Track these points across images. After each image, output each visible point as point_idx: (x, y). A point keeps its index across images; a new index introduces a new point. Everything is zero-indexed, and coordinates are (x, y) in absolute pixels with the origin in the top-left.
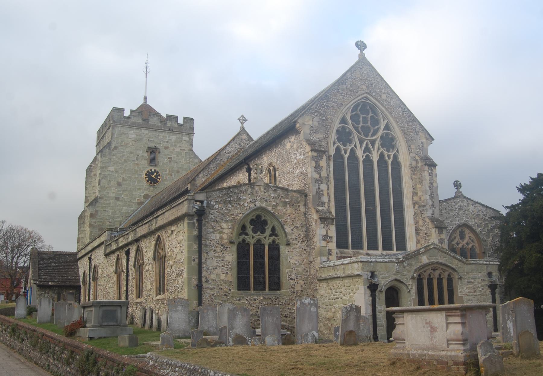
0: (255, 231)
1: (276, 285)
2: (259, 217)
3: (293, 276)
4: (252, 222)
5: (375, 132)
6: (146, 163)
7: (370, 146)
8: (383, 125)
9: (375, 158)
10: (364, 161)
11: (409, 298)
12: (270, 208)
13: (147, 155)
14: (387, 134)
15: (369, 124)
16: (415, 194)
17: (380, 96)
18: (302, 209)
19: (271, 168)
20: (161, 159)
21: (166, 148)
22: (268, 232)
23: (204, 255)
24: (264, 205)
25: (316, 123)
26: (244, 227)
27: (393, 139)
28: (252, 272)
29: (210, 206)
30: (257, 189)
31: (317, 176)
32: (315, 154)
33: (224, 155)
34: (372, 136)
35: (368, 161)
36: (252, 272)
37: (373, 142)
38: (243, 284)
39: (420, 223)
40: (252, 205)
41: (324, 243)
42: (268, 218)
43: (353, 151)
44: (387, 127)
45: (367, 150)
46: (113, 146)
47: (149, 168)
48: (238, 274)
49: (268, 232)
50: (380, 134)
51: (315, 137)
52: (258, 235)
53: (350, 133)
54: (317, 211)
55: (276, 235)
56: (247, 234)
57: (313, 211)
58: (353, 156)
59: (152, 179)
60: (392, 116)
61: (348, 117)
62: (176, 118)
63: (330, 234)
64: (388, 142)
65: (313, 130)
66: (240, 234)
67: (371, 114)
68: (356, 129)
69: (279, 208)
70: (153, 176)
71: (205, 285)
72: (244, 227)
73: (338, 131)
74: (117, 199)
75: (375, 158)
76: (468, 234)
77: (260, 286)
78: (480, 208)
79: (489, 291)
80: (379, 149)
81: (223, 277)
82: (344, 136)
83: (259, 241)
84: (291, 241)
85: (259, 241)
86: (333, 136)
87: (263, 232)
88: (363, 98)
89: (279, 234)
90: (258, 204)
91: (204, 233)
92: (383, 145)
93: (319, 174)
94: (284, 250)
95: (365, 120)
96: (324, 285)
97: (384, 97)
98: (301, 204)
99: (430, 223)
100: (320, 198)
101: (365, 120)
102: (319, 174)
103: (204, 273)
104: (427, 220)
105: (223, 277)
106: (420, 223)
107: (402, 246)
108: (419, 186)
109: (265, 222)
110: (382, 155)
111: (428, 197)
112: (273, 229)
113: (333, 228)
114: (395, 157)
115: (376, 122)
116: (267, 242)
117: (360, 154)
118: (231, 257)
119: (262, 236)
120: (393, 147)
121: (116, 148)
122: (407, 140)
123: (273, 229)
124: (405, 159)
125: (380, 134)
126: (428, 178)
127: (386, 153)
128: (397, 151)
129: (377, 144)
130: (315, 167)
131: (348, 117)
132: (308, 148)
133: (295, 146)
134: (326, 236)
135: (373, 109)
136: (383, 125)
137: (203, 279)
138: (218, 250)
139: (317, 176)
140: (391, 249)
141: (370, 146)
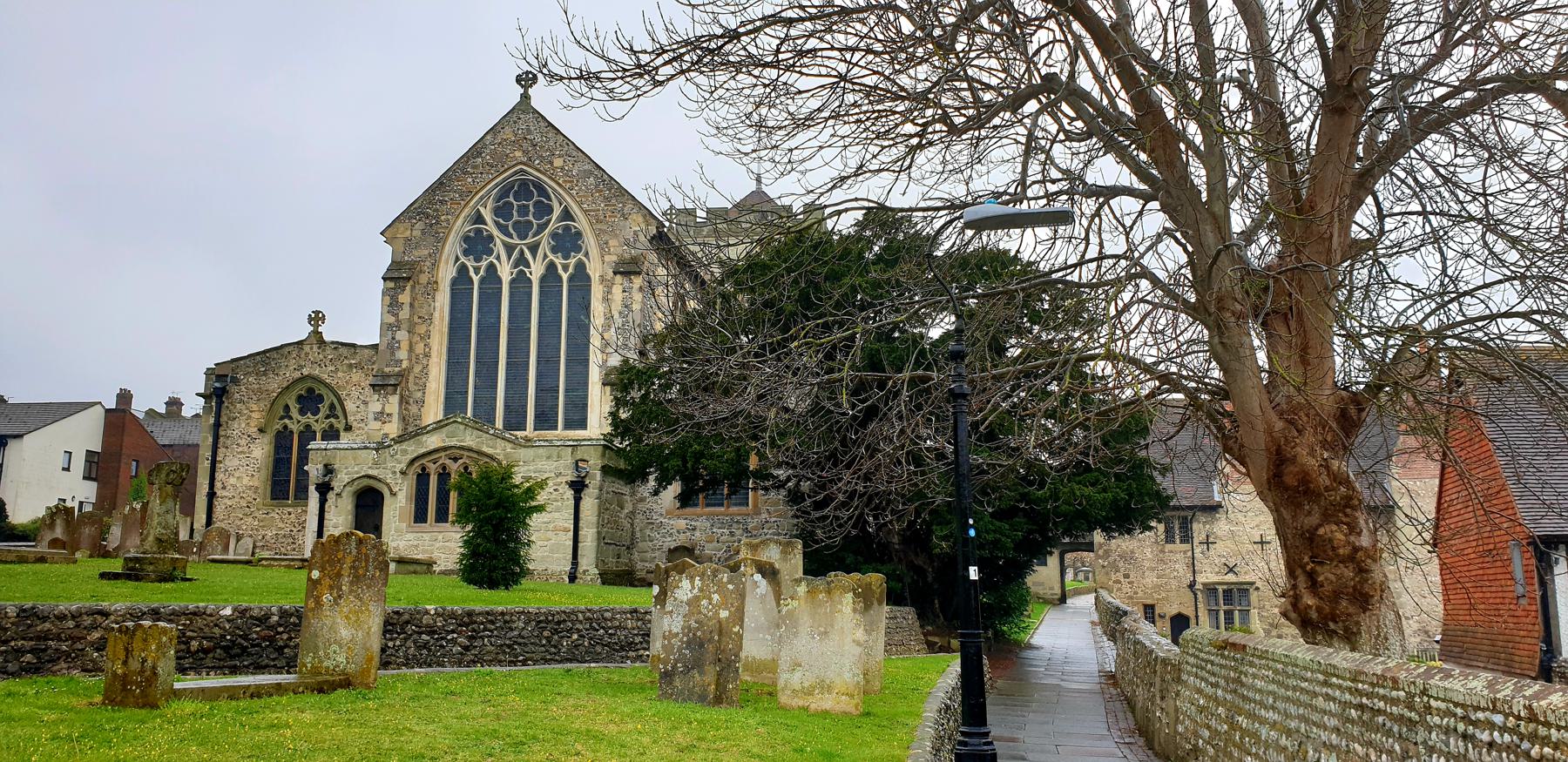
0: (302, 412)
2: (311, 390)
4: (300, 399)
8: (557, 211)
9: (536, 271)
10: (513, 281)
11: (397, 509)
17: (551, 163)
22: (324, 409)
23: (221, 451)
25: (417, 233)
27: (579, 234)
29: (235, 381)
31: (392, 319)
35: (520, 281)
37: (534, 249)
40: (297, 375)
42: (323, 391)
43: (491, 267)
48: (274, 475)
52: (310, 418)
60: (571, 196)
61: (488, 215)
63: (387, 410)
64: (568, 242)
66: (282, 418)
67: (511, 199)
69: (340, 374)
71: (219, 493)
72: (287, 408)
79: (570, 493)
80: (545, 256)
81: (246, 481)
83: (308, 426)
84: (355, 424)
86: (452, 245)
87: (316, 412)
88: (515, 173)
90: (305, 372)
91: (223, 419)
93: (396, 315)
95: (523, 211)
97: (558, 162)
100: (393, 354)
102: (396, 315)
103: (219, 476)
105: (246, 481)
107: (582, 424)
109: (320, 398)
110: (551, 267)
112: (332, 407)
114: (580, 266)
117: (506, 272)
118: (261, 451)
120: (578, 249)
123: (332, 407)
128: (587, 255)
129: (544, 247)
130: (391, 305)
131: (488, 215)
134: (382, 413)
136: (557, 211)
137: (218, 485)
138: (243, 442)
139: (392, 319)
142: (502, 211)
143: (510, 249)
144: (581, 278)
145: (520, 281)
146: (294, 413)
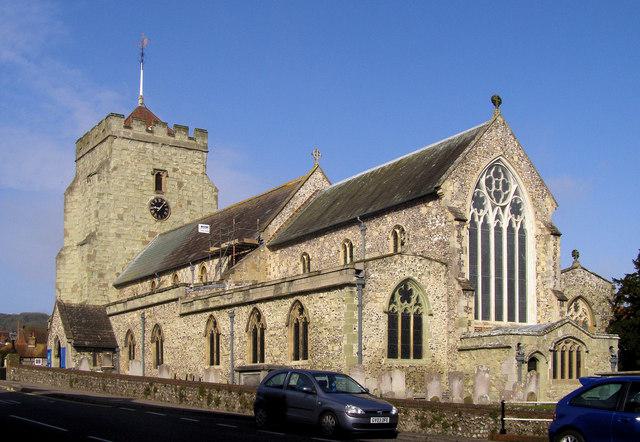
0: (402, 301)
1: (418, 354)
3: (434, 346)
5: (506, 196)
6: (152, 187)
7: (501, 213)
8: (512, 189)
9: (505, 225)
12: (416, 278)
13: (152, 179)
14: (516, 199)
15: (500, 189)
16: (538, 264)
18: (443, 280)
19: (398, 231)
20: (167, 183)
21: (175, 170)
24: (411, 275)
26: (393, 297)
27: (519, 206)
28: (399, 341)
30: (406, 257)
31: (459, 247)
32: (458, 223)
33: (297, 198)
34: (503, 201)
35: (498, 229)
36: (399, 341)
37: (503, 208)
38: (392, 354)
39: (542, 294)
41: (465, 315)
44: (516, 193)
45: (498, 217)
46: (112, 165)
47: (156, 195)
49: (413, 301)
50: (509, 200)
51: (455, 204)
53: (483, 199)
54: (460, 282)
55: (420, 305)
56: (395, 303)
57: (455, 282)
58: (485, 225)
59: (161, 210)
62: (186, 129)
64: (516, 209)
65: (455, 197)
68: (489, 193)
69: (423, 278)
70: (159, 209)
73: (473, 198)
74: (118, 236)
75: (505, 225)
76: (580, 303)
77: (405, 355)
78: (596, 279)
82: (478, 202)
85: (406, 310)
87: (409, 302)
89: (423, 304)
92: (512, 212)
94: (426, 319)
95: (497, 186)
96: (466, 354)
97: (516, 159)
98: (442, 274)
99: (553, 295)
101: (497, 186)
104: (551, 293)
106: (542, 294)
108: (543, 255)
111: (552, 269)
113: (473, 299)
115: (506, 186)
116: (412, 311)
117: (492, 222)
118: (384, 326)
119: (408, 306)
121: (115, 169)
122: (534, 206)
123: (417, 299)
124: (532, 228)
125: (509, 200)
126: (553, 248)
127: (514, 220)
129: (508, 209)
132: (451, 217)
133: (434, 212)
135: (505, 171)
139: (459, 247)
140: (514, 320)
141: (501, 213)
142: (488, 182)
143: (493, 207)
144: (522, 231)
145: (498, 229)
146: (398, 298)
